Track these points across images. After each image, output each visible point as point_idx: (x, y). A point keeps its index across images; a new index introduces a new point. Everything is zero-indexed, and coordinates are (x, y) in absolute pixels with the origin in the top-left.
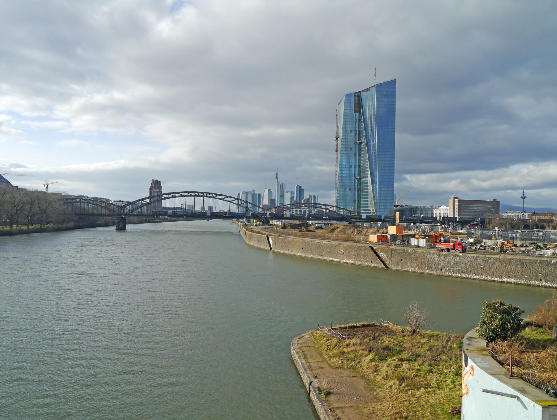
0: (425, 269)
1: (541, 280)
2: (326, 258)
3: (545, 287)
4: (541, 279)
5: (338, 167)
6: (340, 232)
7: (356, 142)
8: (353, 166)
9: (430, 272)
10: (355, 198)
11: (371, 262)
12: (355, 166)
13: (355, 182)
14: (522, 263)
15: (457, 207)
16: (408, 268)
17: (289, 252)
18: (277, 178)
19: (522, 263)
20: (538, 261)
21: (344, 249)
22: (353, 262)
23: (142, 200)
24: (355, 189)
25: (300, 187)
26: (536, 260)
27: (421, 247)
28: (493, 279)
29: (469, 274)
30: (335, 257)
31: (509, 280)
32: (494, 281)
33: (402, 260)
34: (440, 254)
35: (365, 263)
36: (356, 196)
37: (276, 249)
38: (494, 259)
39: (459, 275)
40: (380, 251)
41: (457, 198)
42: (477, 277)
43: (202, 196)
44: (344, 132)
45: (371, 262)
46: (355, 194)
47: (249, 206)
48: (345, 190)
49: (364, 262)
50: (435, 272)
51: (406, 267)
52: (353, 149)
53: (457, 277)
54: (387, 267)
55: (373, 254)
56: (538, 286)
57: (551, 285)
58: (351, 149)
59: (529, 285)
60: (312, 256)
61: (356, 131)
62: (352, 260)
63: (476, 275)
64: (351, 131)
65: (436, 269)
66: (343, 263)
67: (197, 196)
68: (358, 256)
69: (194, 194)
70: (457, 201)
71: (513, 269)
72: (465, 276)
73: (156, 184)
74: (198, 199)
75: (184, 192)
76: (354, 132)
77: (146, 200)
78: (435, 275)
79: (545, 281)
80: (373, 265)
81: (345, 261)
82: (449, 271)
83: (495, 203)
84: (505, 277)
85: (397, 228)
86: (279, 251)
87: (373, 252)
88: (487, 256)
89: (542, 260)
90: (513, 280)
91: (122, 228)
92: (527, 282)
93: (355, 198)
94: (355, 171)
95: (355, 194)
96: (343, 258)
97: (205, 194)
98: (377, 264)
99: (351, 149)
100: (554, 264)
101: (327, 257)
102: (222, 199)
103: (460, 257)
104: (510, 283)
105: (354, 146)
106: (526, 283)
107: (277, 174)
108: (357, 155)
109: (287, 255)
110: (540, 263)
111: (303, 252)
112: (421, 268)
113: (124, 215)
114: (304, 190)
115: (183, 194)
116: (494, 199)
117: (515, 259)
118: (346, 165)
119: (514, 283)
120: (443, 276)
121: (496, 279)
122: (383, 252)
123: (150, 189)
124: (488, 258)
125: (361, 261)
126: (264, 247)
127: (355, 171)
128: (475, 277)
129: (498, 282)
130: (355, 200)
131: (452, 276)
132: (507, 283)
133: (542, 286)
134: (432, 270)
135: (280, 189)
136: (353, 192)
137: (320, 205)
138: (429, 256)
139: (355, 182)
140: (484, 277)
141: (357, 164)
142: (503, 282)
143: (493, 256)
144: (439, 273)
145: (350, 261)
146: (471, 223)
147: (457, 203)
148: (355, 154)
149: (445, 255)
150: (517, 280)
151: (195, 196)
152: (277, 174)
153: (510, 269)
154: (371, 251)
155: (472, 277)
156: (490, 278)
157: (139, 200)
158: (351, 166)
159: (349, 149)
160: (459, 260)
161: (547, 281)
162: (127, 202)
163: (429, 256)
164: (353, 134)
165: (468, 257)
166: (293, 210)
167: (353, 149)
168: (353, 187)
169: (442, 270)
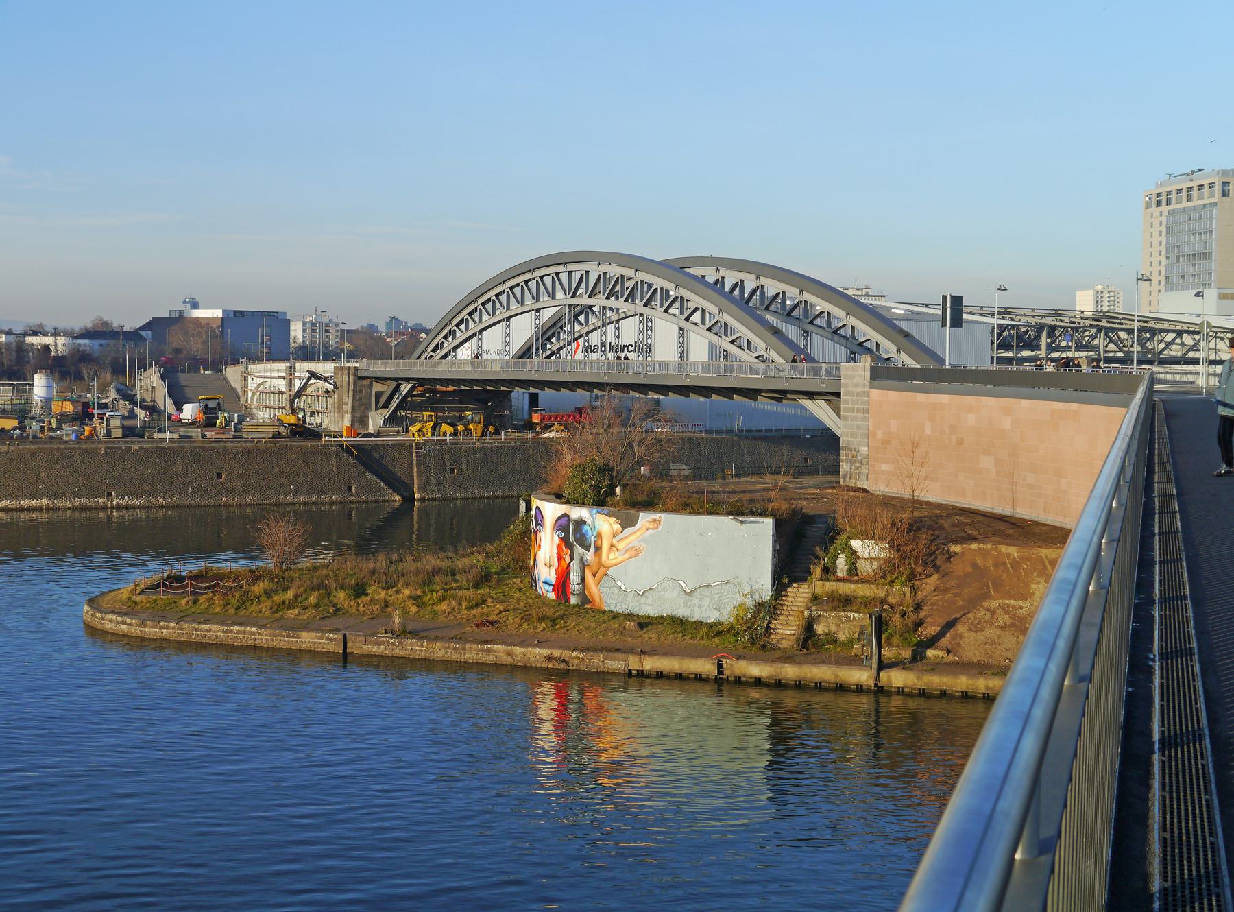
1: (109, 495)
4: (110, 491)
20: (100, 449)
26: (96, 449)
59: (82, 509)
71: (43, 475)
79: (117, 497)
84: (25, 497)
89: (108, 448)
90: (44, 502)
92: (77, 502)
100: (135, 453)
106: (77, 504)
110: (106, 453)
117: (46, 449)
119: (48, 509)
133: (112, 508)
142: (22, 510)
150: (55, 501)
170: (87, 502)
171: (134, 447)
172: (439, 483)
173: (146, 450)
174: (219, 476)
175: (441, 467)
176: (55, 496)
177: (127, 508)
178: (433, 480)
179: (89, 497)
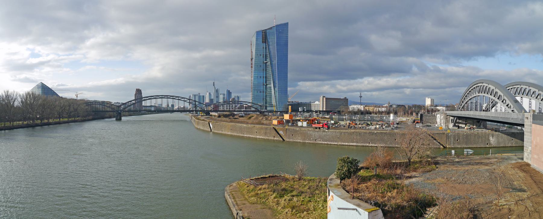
0: (306, 140)
1: (369, 143)
2: (246, 135)
3: (371, 146)
5: (253, 78)
6: (254, 119)
7: (263, 62)
8: (262, 77)
9: (309, 142)
10: (263, 97)
11: (274, 137)
12: (263, 77)
13: (263, 87)
14: (360, 134)
15: (325, 102)
16: (296, 140)
17: (223, 132)
18: (214, 85)
19: (360, 134)
21: (257, 130)
22: (263, 137)
23: (131, 101)
24: (263, 91)
25: (229, 91)
27: (304, 127)
28: (344, 144)
29: (331, 141)
30: (252, 135)
31: (353, 144)
32: (345, 145)
33: (293, 135)
34: (315, 131)
35: (270, 138)
36: (264, 96)
37: (215, 130)
38: (345, 132)
39: (326, 143)
40: (280, 130)
41: (324, 97)
42: (336, 143)
43: (167, 98)
44: (256, 55)
45: (274, 137)
46: (263, 95)
47: (197, 103)
48: (257, 93)
49: (269, 137)
50: (312, 142)
51: (295, 140)
52: (262, 66)
53: (325, 144)
54: (283, 140)
55: (275, 132)
56: (368, 146)
57: (374, 145)
58: (261, 66)
59: (363, 146)
60: (237, 134)
61: (263, 55)
62: (262, 136)
63: (335, 142)
64: (261, 55)
65: (313, 140)
66: (257, 138)
67: (164, 98)
68: (266, 134)
69: (162, 97)
70: (324, 98)
72: (329, 143)
73: (139, 92)
74: (165, 100)
75: (156, 96)
76: (262, 55)
77: (133, 102)
78: (312, 143)
79: (371, 143)
80: (275, 139)
81: (258, 137)
82: (320, 141)
83: (346, 100)
84: (351, 142)
85: (290, 116)
86: (216, 131)
87: (275, 131)
88: (341, 131)
90: (355, 144)
91: (119, 119)
92: (362, 144)
93: (263, 97)
94: (263, 80)
95: (263, 95)
96: (257, 135)
97: (168, 97)
98: (278, 138)
99: (261, 66)
100: (376, 134)
101: (247, 135)
102: (179, 100)
103: (326, 132)
104: (354, 146)
105: (262, 65)
107: (214, 83)
108: (265, 70)
109: (221, 134)
111: (231, 132)
112: (304, 139)
113: (120, 111)
114: (231, 92)
115: (155, 97)
116: (345, 98)
118: (257, 76)
119: (356, 146)
120: (317, 143)
121: (346, 144)
122: (281, 130)
123: (135, 95)
124: (342, 132)
125: (268, 136)
126: (207, 130)
127: (263, 80)
128: (335, 143)
129: (347, 145)
130: (263, 99)
131: (322, 144)
132: (352, 145)
134: (311, 141)
135: (216, 92)
136: (262, 94)
137: (241, 102)
138: (309, 132)
139: (263, 87)
140: (340, 143)
141: (264, 76)
142: (350, 145)
143: (345, 131)
144: (314, 142)
145: (261, 137)
146: (333, 112)
147: (325, 100)
148: (263, 70)
149: (318, 131)
151: (162, 98)
152: (214, 83)
153: (354, 137)
154: (274, 130)
155: (333, 143)
156: (343, 144)
157: (129, 102)
158: (261, 77)
159: (259, 66)
160: (326, 134)
161: (372, 143)
162: (122, 103)
163: (309, 132)
164: (262, 57)
165: (331, 132)
166: (225, 105)
167: (262, 66)
168: (262, 90)
169: (316, 140)
170: (365, 145)
171: (375, 132)
172: (454, 143)
173: (378, 133)
174: (395, 140)
175: (454, 138)
176: (357, 143)
177: (373, 146)
178: (452, 143)
179: (365, 143)
